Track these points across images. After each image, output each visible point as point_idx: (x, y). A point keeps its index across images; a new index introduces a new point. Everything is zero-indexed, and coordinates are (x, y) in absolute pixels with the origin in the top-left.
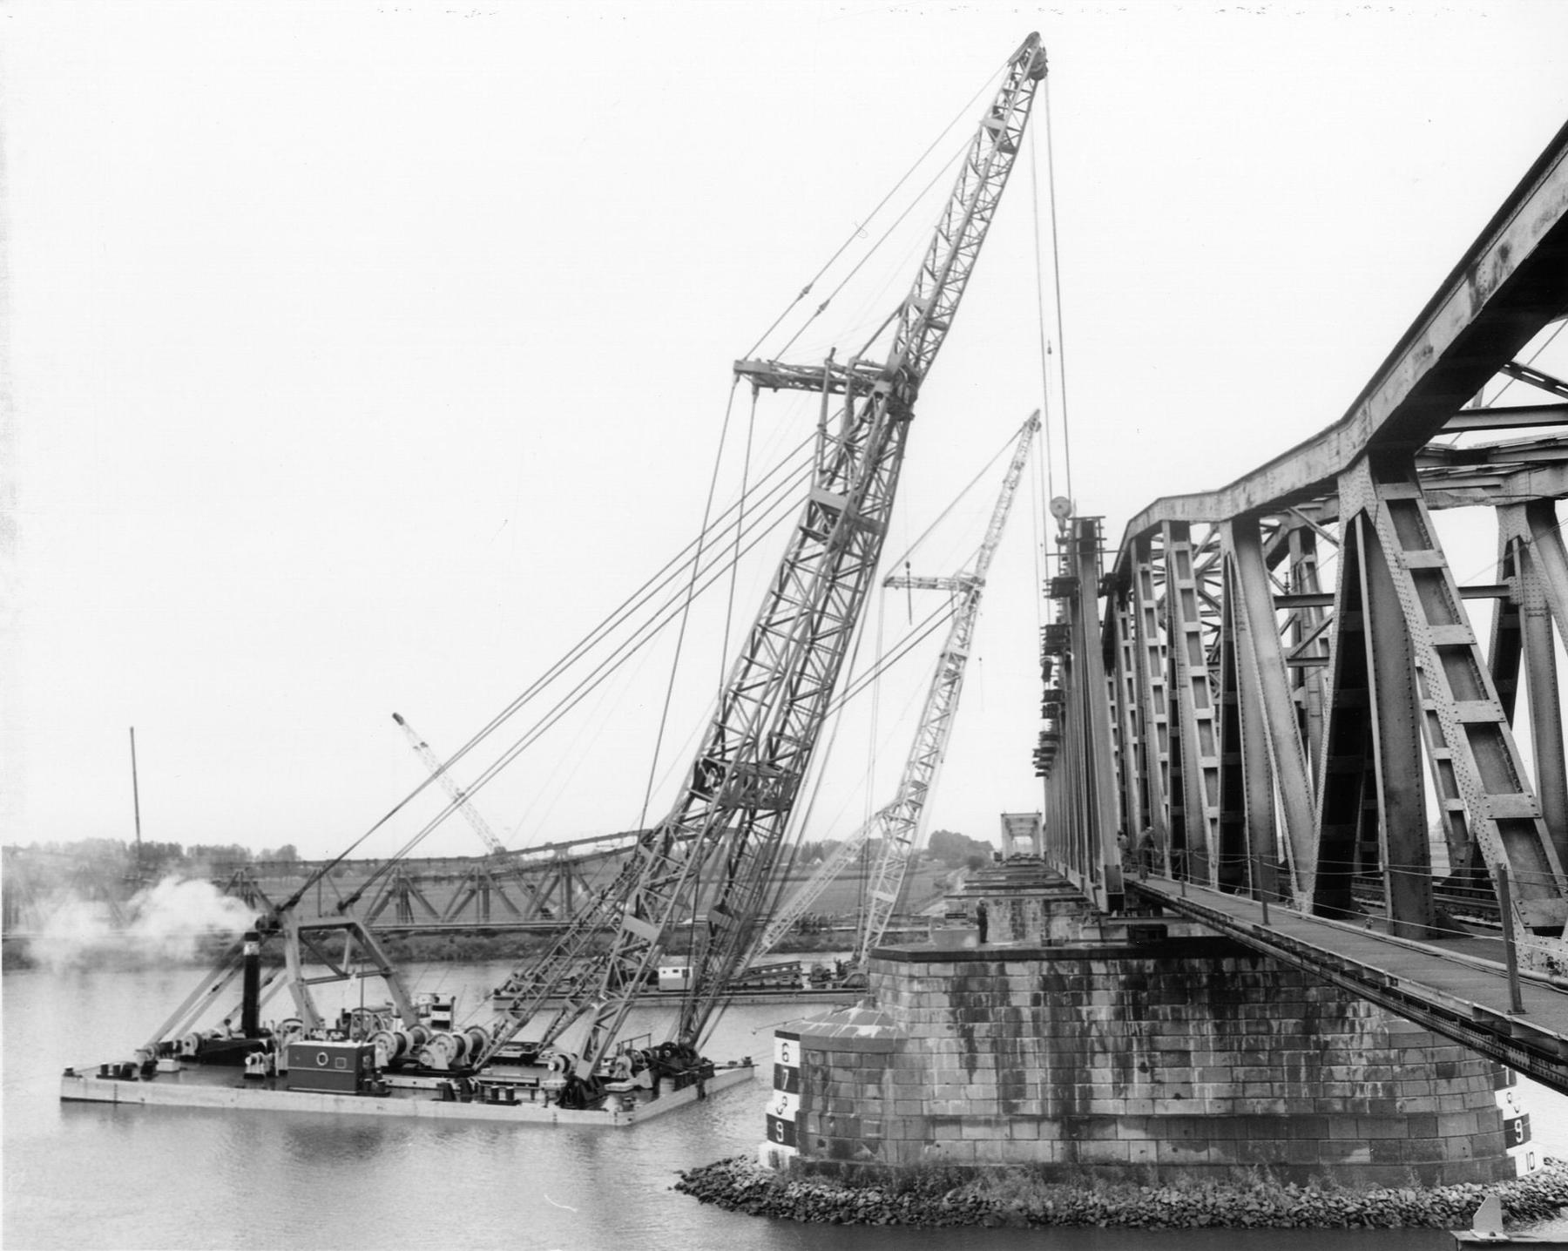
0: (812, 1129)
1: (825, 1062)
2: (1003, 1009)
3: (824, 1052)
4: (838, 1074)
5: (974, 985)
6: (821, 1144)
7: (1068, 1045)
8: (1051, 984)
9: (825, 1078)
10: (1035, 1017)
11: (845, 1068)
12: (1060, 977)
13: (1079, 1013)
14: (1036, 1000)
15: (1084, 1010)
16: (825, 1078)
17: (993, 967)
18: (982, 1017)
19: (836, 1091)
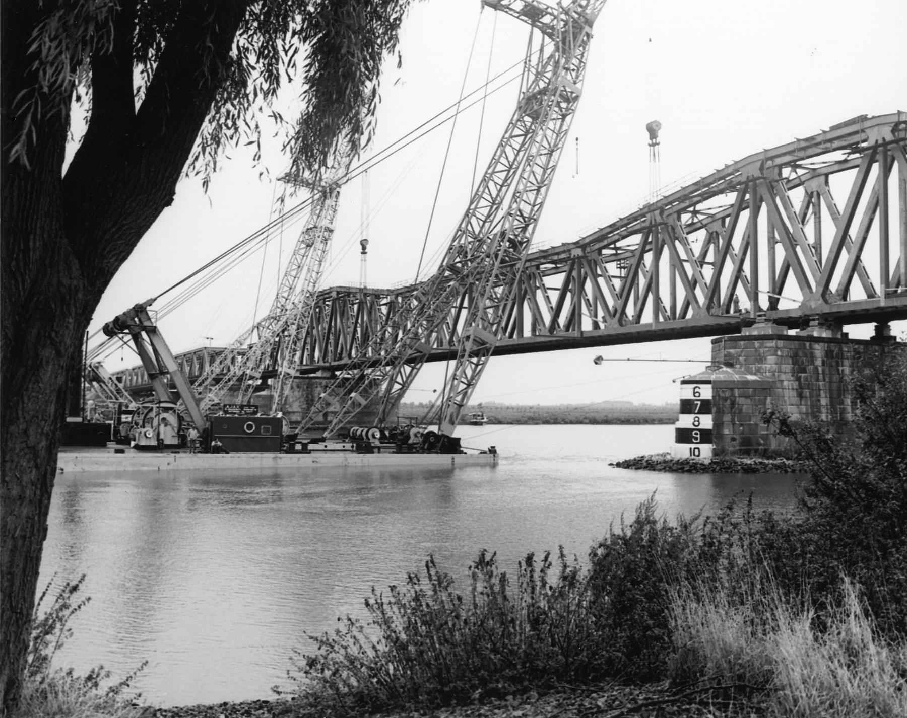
0: (726, 432)
1: (733, 395)
2: (812, 367)
3: (732, 389)
4: (741, 401)
5: (801, 354)
6: (733, 439)
7: (835, 386)
8: (829, 354)
9: (733, 404)
10: (824, 373)
11: (746, 397)
12: (832, 352)
13: (838, 370)
14: (823, 363)
15: (841, 368)
16: (733, 404)
17: (808, 344)
18: (804, 371)
19: (740, 411)
